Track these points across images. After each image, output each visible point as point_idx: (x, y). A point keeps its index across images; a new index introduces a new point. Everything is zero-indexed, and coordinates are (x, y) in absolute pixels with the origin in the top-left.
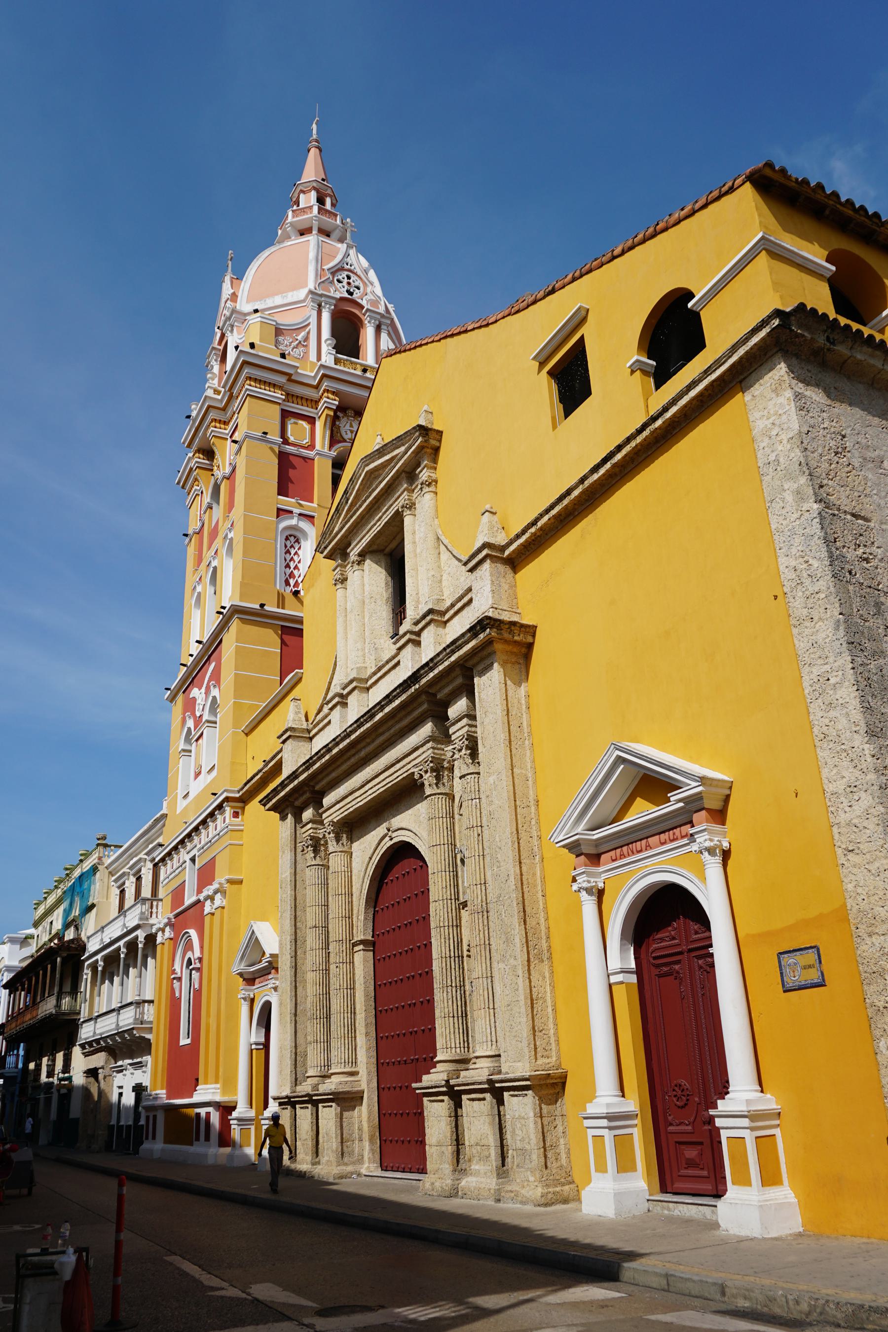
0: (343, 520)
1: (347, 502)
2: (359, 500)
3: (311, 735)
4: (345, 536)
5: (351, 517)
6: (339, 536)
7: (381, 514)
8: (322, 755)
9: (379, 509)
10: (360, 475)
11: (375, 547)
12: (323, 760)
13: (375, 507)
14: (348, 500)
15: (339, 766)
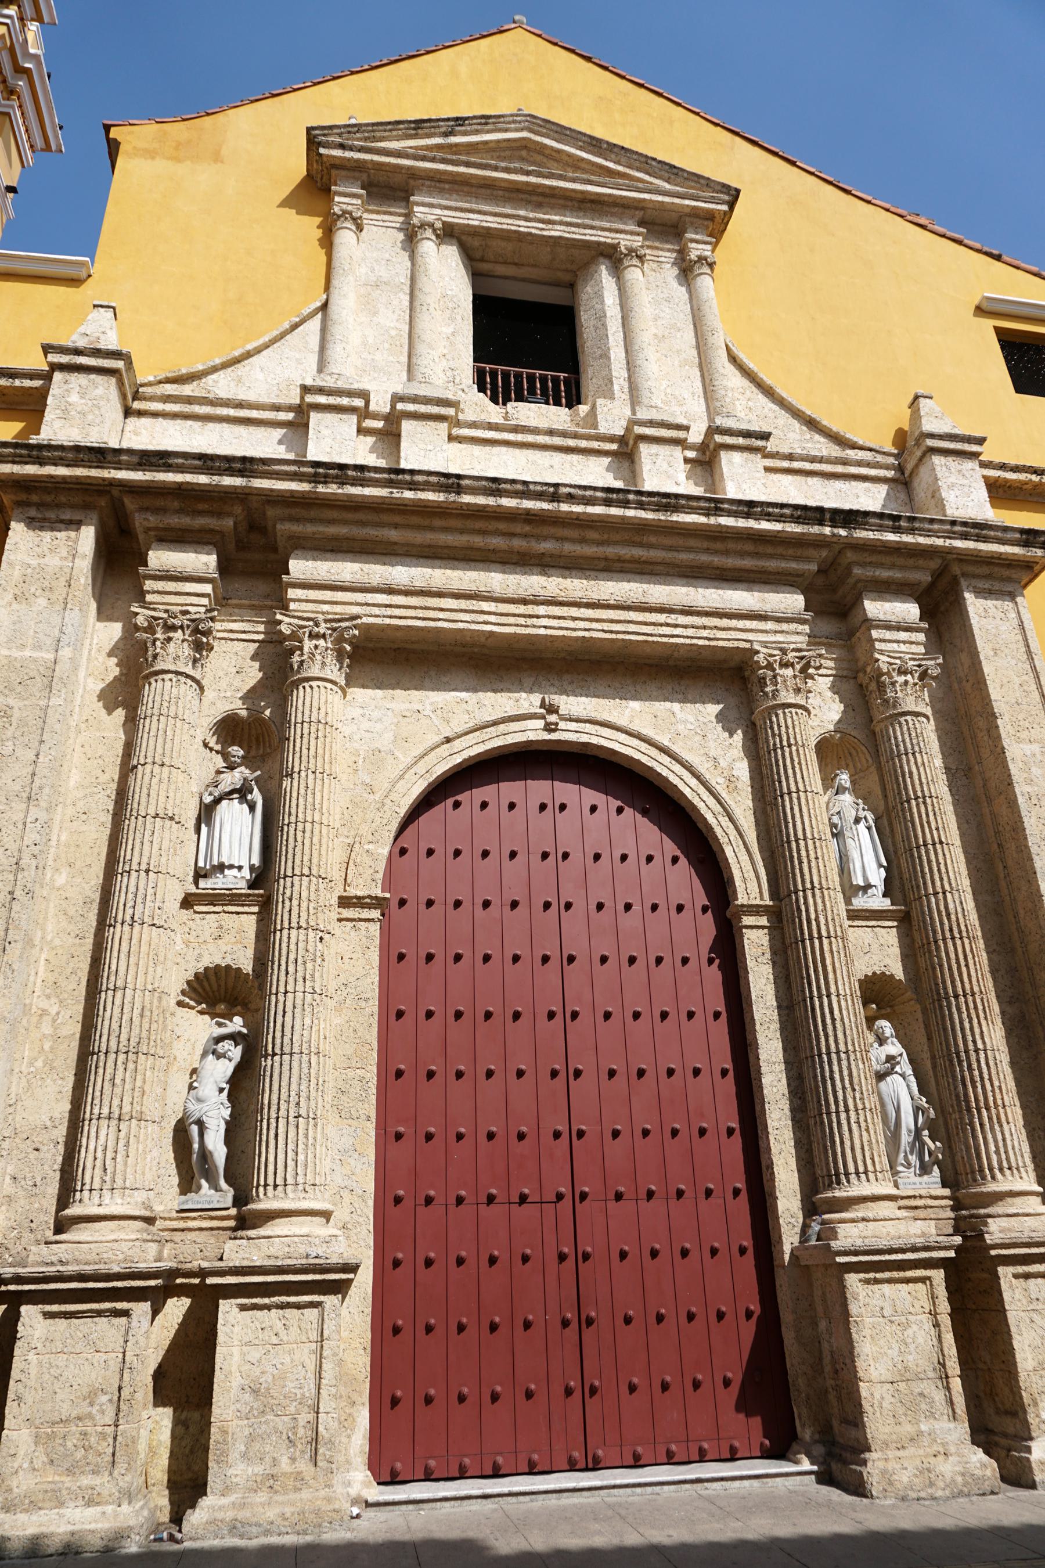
0: (421, 148)
1: (446, 135)
2: (468, 154)
3: (137, 405)
4: (413, 174)
5: (444, 161)
6: (376, 158)
7: (557, 218)
8: (400, 482)
9: (539, 206)
10: (506, 130)
11: (476, 243)
12: (397, 494)
13: (535, 198)
14: (451, 133)
15: (432, 529)
